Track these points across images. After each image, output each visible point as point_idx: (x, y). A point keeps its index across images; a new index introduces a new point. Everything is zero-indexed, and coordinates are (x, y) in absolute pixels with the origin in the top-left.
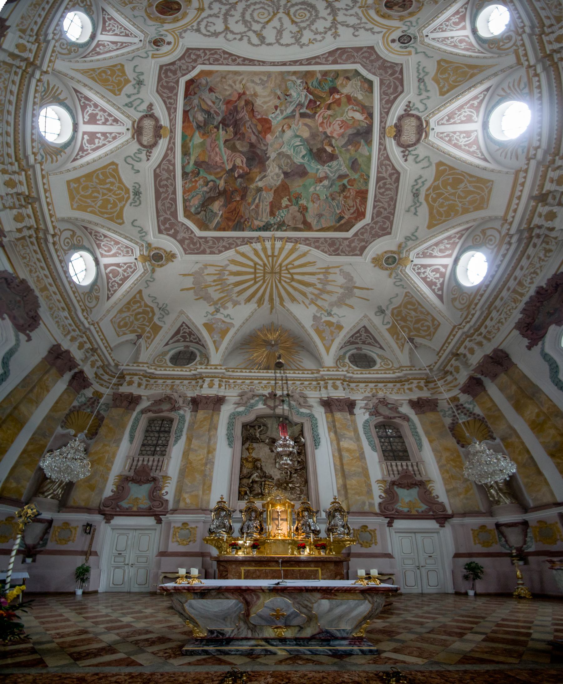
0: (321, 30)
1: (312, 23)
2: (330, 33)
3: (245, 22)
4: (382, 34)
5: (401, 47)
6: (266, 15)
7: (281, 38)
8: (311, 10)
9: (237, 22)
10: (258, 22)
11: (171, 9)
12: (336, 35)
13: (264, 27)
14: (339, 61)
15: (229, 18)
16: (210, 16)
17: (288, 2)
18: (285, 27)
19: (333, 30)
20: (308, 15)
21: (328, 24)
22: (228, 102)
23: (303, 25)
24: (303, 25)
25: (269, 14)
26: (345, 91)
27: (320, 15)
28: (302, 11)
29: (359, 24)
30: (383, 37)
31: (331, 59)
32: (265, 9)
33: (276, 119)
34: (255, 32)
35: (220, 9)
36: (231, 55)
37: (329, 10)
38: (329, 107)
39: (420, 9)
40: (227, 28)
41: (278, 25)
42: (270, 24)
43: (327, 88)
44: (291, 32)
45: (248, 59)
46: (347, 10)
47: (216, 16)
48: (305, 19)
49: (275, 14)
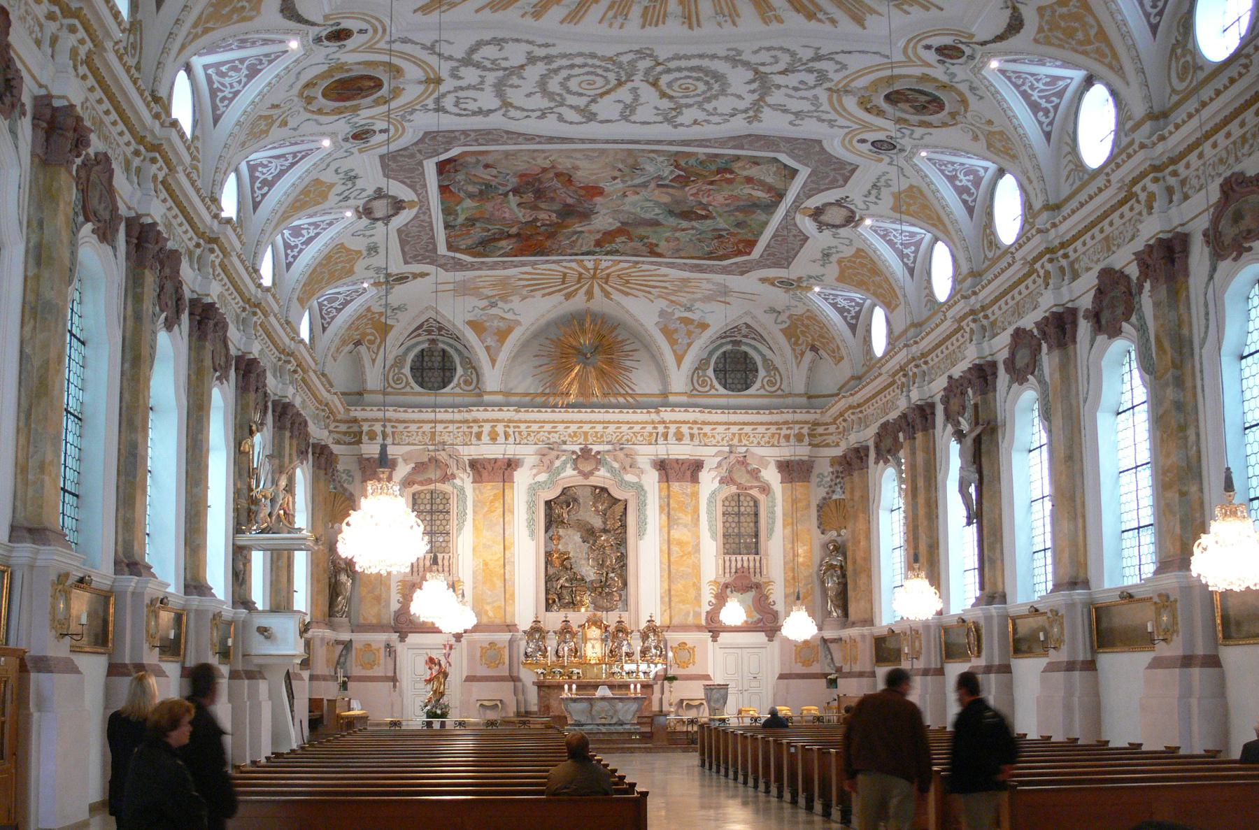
1: (708, 100)
2: (741, 116)
3: (550, 95)
4: (847, 130)
5: (870, 151)
6: (600, 82)
7: (633, 111)
8: (712, 81)
9: (528, 95)
10: (581, 95)
14: (746, 147)
16: (461, 88)
17: (659, 64)
18: (642, 100)
19: (751, 113)
20: (702, 87)
21: (742, 105)
22: (521, 176)
26: (745, 173)
27: (729, 91)
28: (690, 81)
29: (808, 112)
30: (847, 134)
31: (731, 144)
32: (598, 75)
34: (571, 107)
35: (480, 76)
36: (520, 134)
37: (755, 86)
38: (712, 183)
39: (945, 125)
40: (507, 105)
41: (628, 99)
42: (606, 98)
43: (714, 168)
44: (656, 108)
45: (558, 138)
46: (796, 89)
48: (692, 93)
49: (620, 84)
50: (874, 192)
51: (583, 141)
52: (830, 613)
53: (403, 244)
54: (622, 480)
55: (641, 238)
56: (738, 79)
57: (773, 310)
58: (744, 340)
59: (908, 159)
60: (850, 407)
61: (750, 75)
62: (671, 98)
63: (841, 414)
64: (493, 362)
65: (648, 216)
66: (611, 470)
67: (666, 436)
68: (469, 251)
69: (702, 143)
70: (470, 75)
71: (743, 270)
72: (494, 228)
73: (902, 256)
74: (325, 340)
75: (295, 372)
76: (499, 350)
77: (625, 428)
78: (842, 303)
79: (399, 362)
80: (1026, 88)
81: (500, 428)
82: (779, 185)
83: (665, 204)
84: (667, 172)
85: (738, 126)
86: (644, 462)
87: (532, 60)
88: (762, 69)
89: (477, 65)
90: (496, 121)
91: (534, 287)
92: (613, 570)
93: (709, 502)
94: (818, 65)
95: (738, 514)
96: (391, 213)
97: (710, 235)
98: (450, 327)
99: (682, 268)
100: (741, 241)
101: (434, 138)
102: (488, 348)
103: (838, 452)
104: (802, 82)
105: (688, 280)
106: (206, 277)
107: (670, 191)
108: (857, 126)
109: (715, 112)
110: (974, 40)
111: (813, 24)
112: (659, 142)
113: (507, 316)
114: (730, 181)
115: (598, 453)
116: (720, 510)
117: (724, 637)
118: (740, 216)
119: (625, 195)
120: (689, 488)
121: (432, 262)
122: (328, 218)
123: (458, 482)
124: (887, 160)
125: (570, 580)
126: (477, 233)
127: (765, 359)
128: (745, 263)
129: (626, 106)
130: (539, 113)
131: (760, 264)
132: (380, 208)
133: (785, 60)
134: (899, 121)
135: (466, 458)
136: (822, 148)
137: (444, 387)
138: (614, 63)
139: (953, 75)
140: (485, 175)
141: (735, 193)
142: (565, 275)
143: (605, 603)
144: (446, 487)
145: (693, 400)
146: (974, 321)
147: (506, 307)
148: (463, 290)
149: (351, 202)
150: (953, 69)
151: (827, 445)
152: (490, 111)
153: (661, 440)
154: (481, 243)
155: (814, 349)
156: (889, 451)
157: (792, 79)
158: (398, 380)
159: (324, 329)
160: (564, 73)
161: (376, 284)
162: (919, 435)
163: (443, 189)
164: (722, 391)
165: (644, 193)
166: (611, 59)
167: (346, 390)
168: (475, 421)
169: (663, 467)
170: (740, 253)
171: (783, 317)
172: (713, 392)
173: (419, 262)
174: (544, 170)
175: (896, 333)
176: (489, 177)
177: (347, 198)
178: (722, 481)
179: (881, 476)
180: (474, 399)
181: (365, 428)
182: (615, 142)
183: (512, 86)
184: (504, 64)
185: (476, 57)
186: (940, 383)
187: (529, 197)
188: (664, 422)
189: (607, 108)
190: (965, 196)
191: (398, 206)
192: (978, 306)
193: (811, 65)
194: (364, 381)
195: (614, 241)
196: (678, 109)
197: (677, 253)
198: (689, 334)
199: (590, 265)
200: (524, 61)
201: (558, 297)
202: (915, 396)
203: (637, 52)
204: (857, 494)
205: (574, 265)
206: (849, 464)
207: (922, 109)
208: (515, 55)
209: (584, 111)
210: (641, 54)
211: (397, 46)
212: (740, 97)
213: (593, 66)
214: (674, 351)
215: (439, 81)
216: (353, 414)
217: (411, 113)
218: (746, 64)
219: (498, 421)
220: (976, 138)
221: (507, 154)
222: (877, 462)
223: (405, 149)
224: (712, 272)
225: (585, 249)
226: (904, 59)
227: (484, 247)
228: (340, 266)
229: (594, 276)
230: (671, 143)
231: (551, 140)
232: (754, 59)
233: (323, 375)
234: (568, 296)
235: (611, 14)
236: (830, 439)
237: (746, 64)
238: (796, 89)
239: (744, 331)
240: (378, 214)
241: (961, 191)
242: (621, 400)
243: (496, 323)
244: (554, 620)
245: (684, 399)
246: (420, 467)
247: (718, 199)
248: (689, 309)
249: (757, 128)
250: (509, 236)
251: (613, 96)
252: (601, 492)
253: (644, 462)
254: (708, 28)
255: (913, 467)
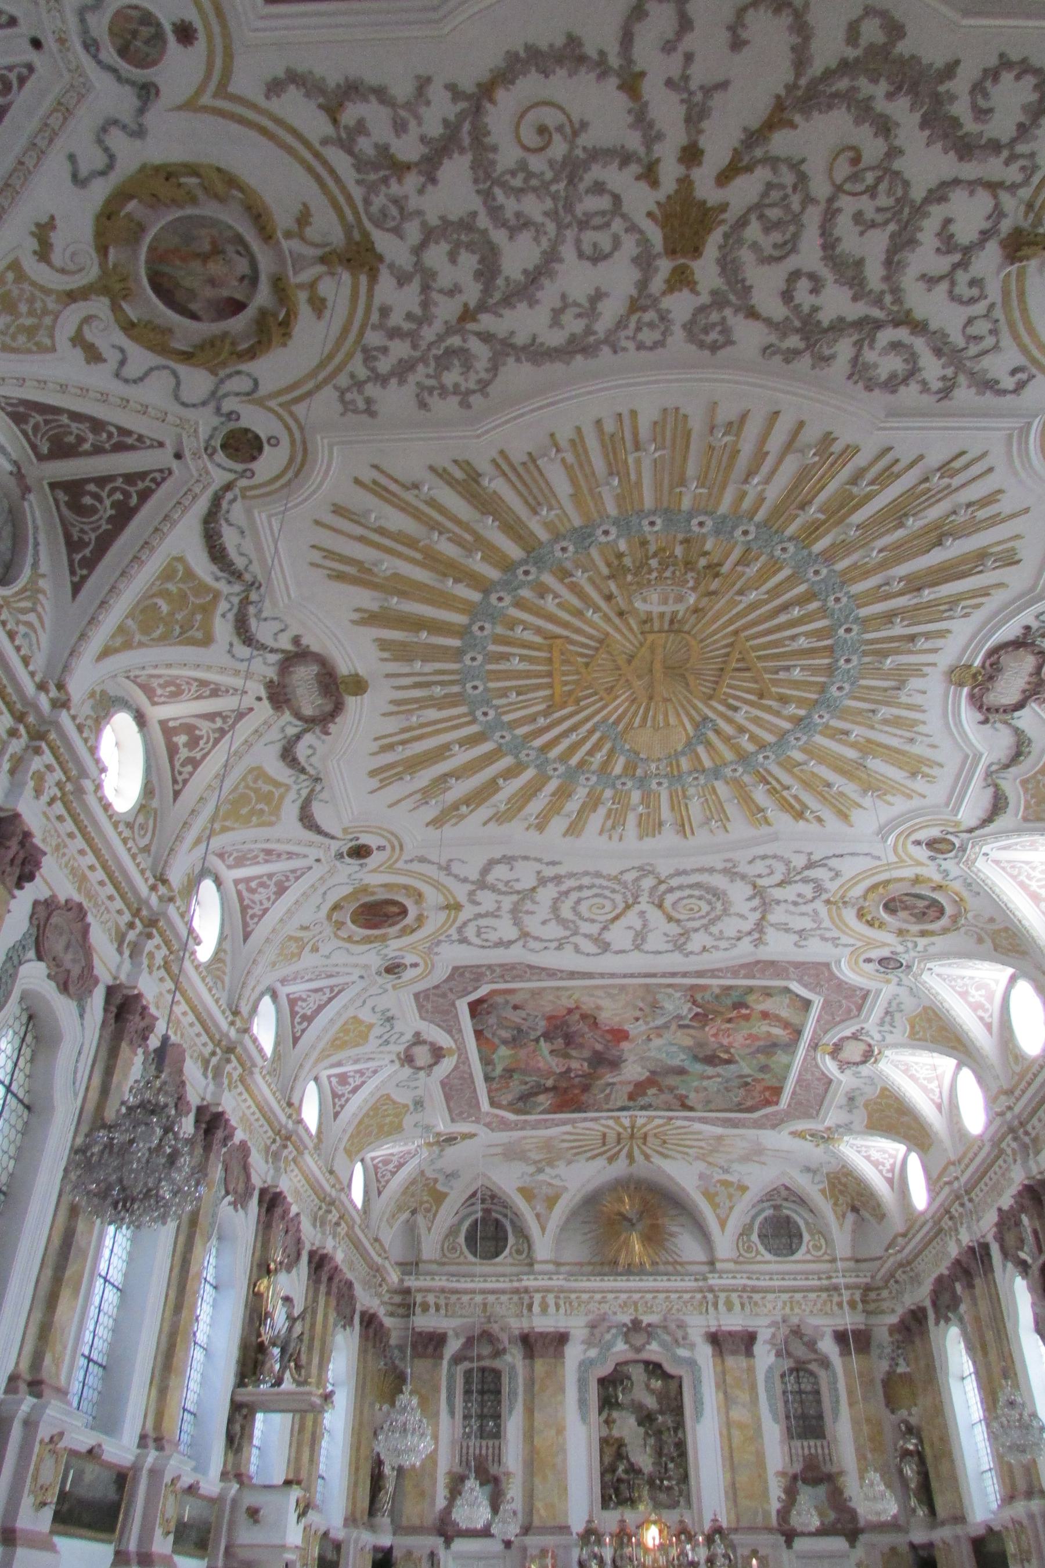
0: (731, 932)
1: (712, 922)
2: (747, 940)
3: (563, 922)
6: (608, 905)
7: (643, 940)
9: (544, 923)
10: (593, 921)
11: (387, 916)
12: (759, 942)
13: (605, 928)
15: (527, 920)
16: (479, 916)
17: (661, 882)
18: (651, 926)
19: (756, 935)
20: (705, 908)
21: (748, 926)
22: (550, 1018)
23: (691, 925)
24: (691, 925)
25: (615, 907)
27: (732, 911)
33: (635, 1029)
34: (586, 936)
37: (756, 902)
38: (730, 1021)
40: (525, 935)
41: (638, 924)
42: (618, 923)
43: (729, 1002)
46: (795, 904)
47: (494, 915)
49: (628, 907)
50: (888, 1019)
51: (602, 975)
52: (914, 1511)
53: (448, 1098)
54: (674, 1355)
55: (671, 1089)
56: (738, 893)
57: (808, 1170)
58: (785, 1204)
59: (915, 977)
60: (901, 1265)
61: (749, 891)
62: (678, 921)
63: (892, 1276)
64: (543, 1229)
65: (676, 1062)
66: (663, 1344)
67: (716, 1305)
68: (512, 1107)
69: (713, 973)
70: (487, 900)
71: (775, 1123)
72: (532, 1079)
73: (925, 1090)
74: (382, 1204)
75: (337, 1224)
76: (548, 1219)
77: (674, 1296)
78: (875, 1155)
79: (453, 1231)
80: (1022, 878)
81: (551, 1299)
82: (795, 1020)
83: (689, 1048)
84: (686, 1010)
85: (745, 951)
86: (696, 1335)
87: (543, 881)
88: (760, 882)
89: (493, 889)
90: (515, 954)
91: (579, 1151)
92: (672, 1460)
93: (768, 1379)
94: (812, 873)
95: (800, 1392)
96: (431, 1061)
97: (735, 1083)
98: (500, 1194)
99: (713, 1122)
100: (767, 1088)
101: (462, 975)
102: (538, 1216)
103: (894, 1319)
104: (799, 895)
105: (720, 1138)
106: (219, 1085)
107: (692, 1032)
108: (859, 944)
109: (721, 937)
110: (963, 828)
111: (801, 823)
112: (673, 975)
113: (554, 1182)
114: (747, 1018)
115: (649, 1325)
116: (779, 1388)
117: (799, 1544)
118: (762, 1058)
119: (649, 1039)
120: (742, 1362)
121: (477, 1121)
122: (371, 1065)
123: (508, 1358)
124: (895, 980)
125: (626, 1472)
126: (516, 1087)
127: (807, 1223)
128: (774, 1114)
129: (637, 934)
130: (555, 944)
131: (789, 1116)
132: (422, 1055)
133: (780, 869)
134: (900, 933)
135: (517, 1332)
136: (831, 973)
137: (497, 1255)
138: (619, 882)
139: (946, 873)
140: (516, 1017)
141: (754, 1031)
142: (604, 1135)
143: (662, 1497)
144: (497, 1364)
145: (738, 1267)
146: (1015, 1139)
147: (552, 1172)
148: (512, 1154)
149: (391, 1047)
150: (946, 865)
151: (882, 1312)
152: (511, 943)
153: (711, 1309)
154: (520, 1098)
155: (855, 1209)
156: (948, 1307)
157: (789, 893)
158: (454, 1249)
159: (380, 1193)
160: (574, 896)
161: (430, 1145)
162: (978, 1282)
163: (478, 1034)
164: (768, 1256)
165: (668, 1036)
166: (616, 879)
167: (400, 1260)
168: (526, 1290)
169: (715, 1339)
170: (768, 1103)
171: (817, 1178)
172: (759, 1258)
173: (464, 1120)
174: (570, 1011)
175: (935, 1175)
176: (518, 1020)
177: (387, 1042)
178: (778, 1354)
179: (944, 1338)
180: (526, 1269)
181: (419, 1299)
182: (632, 976)
183: (528, 912)
184: (518, 886)
185: (490, 878)
186: (991, 1218)
187: (560, 1042)
188: (711, 1290)
189: (619, 935)
190: (980, 1013)
191: (438, 1053)
192: (1016, 1123)
193: (806, 873)
194: (419, 1250)
195: (645, 1094)
196: (686, 934)
197: (708, 1105)
198: (730, 1197)
199: (627, 1122)
200: (534, 883)
201: (601, 1162)
202: (965, 1238)
203: (641, 868)
204: (922, 1363)
205: (611, 1123)
206: (908, 1329)
207: (921, 916)
208: (525, 876)
209: (597, 940)
210: (645, 871)
211: (416, 867)
212: (742, 916)
213: (601, 887)
214: (718, 1216)
215: (458, 907)
216: (406, 1284)
217: (439, 943)
218: (743, 877)
219: (548, 1290)
220: (980, 940)
221: (535, 993)
222: (937, 1323)
223: (436, 987)
224: (744, 1126)
225: (619, 1104)
226: (893, 859)
227: (523, 1102)
228: (388, 1120)
229: (632, 1136)
230: (685, 975)
231: (572, 975)
232: (751, 870)
233: (377, 1240)
234: (611, 1160)
235: (609, 823)
236: (885, 1305)
237: (743, 877)
238: (795, 904)
239: (784, 1193)
240: (420, 1063)
241: (976, 1007)
242: (670, 1268)
243: (545, 1189)
244: (610, 1520)
245: (731, 1266)
246: (469, 1342)
247: (737, 1039)
248: (726, 1171)
249: (765, 953)
250: (547, 1090)
251: (623, 922)
252: (654, 1369)
253: (696, 1335)
254: (702, 837)
255: (977, 1319)
